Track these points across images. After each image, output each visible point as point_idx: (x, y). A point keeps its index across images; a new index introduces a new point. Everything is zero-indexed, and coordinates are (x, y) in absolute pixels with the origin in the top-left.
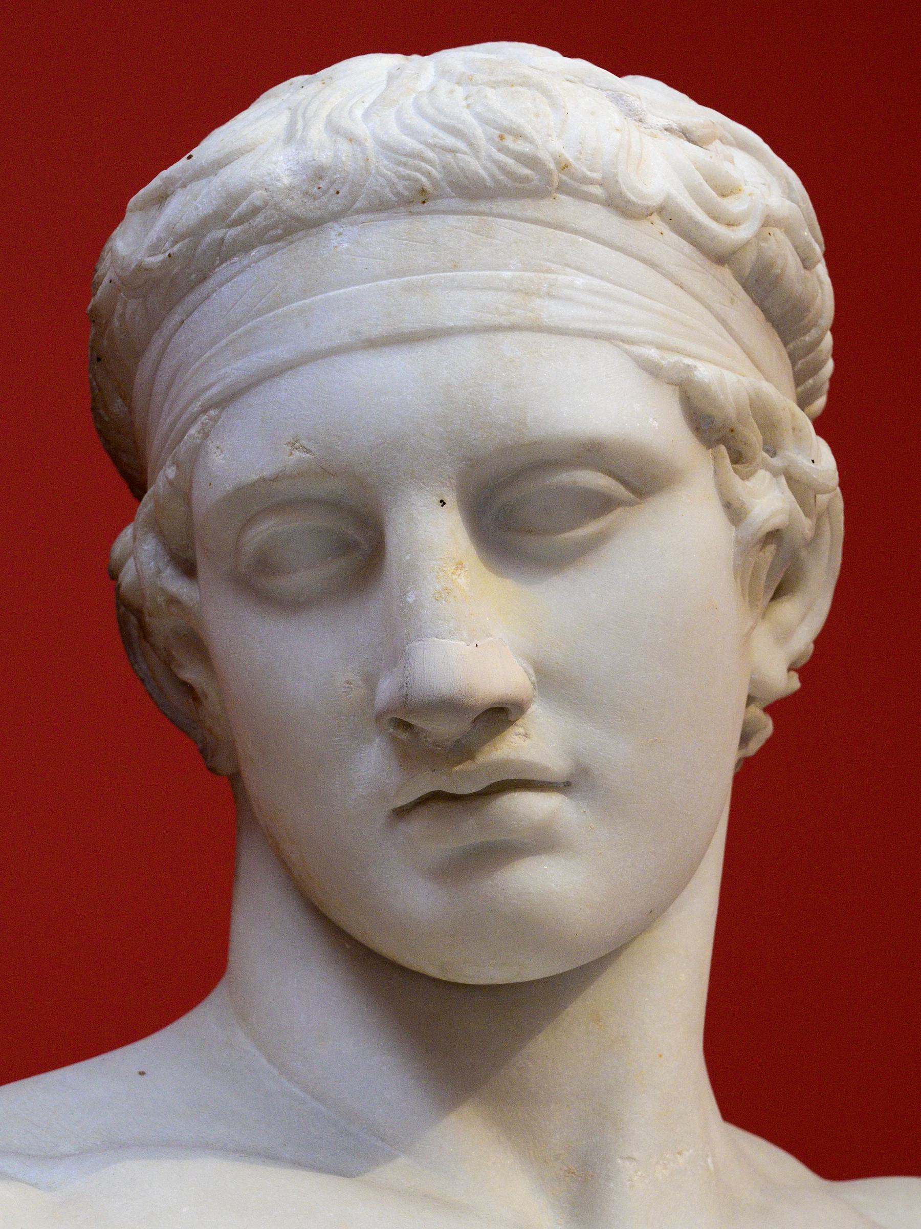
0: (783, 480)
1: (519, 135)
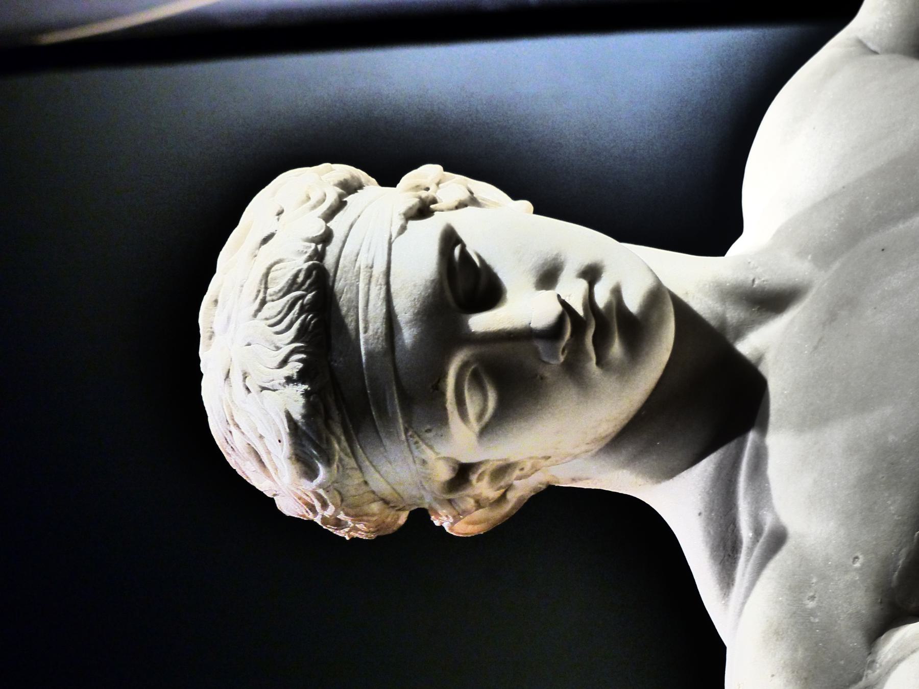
1: (296, 276)
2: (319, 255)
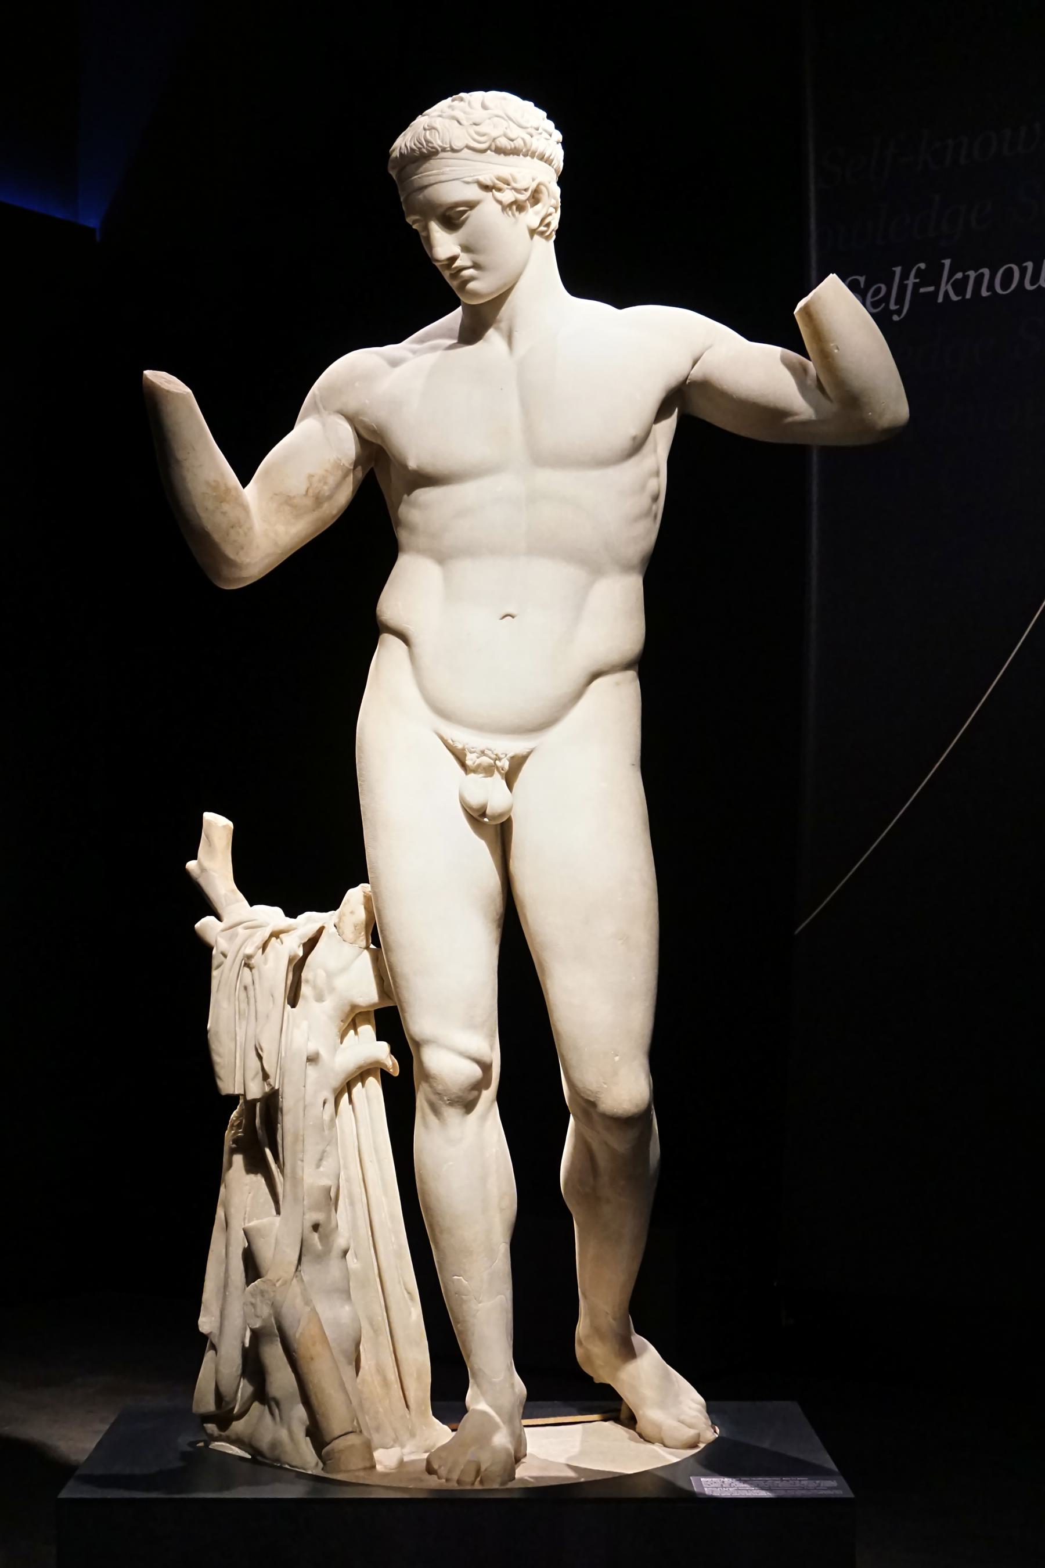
0: (513, 191)
1: (432, 143)
2: (444, 150)
